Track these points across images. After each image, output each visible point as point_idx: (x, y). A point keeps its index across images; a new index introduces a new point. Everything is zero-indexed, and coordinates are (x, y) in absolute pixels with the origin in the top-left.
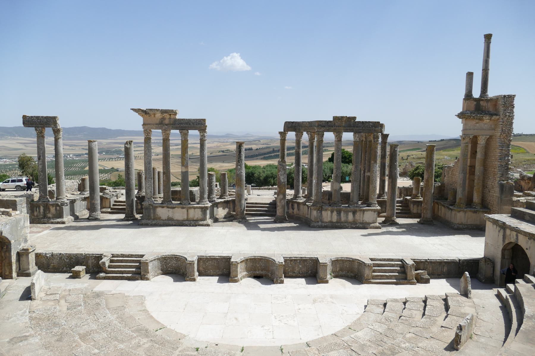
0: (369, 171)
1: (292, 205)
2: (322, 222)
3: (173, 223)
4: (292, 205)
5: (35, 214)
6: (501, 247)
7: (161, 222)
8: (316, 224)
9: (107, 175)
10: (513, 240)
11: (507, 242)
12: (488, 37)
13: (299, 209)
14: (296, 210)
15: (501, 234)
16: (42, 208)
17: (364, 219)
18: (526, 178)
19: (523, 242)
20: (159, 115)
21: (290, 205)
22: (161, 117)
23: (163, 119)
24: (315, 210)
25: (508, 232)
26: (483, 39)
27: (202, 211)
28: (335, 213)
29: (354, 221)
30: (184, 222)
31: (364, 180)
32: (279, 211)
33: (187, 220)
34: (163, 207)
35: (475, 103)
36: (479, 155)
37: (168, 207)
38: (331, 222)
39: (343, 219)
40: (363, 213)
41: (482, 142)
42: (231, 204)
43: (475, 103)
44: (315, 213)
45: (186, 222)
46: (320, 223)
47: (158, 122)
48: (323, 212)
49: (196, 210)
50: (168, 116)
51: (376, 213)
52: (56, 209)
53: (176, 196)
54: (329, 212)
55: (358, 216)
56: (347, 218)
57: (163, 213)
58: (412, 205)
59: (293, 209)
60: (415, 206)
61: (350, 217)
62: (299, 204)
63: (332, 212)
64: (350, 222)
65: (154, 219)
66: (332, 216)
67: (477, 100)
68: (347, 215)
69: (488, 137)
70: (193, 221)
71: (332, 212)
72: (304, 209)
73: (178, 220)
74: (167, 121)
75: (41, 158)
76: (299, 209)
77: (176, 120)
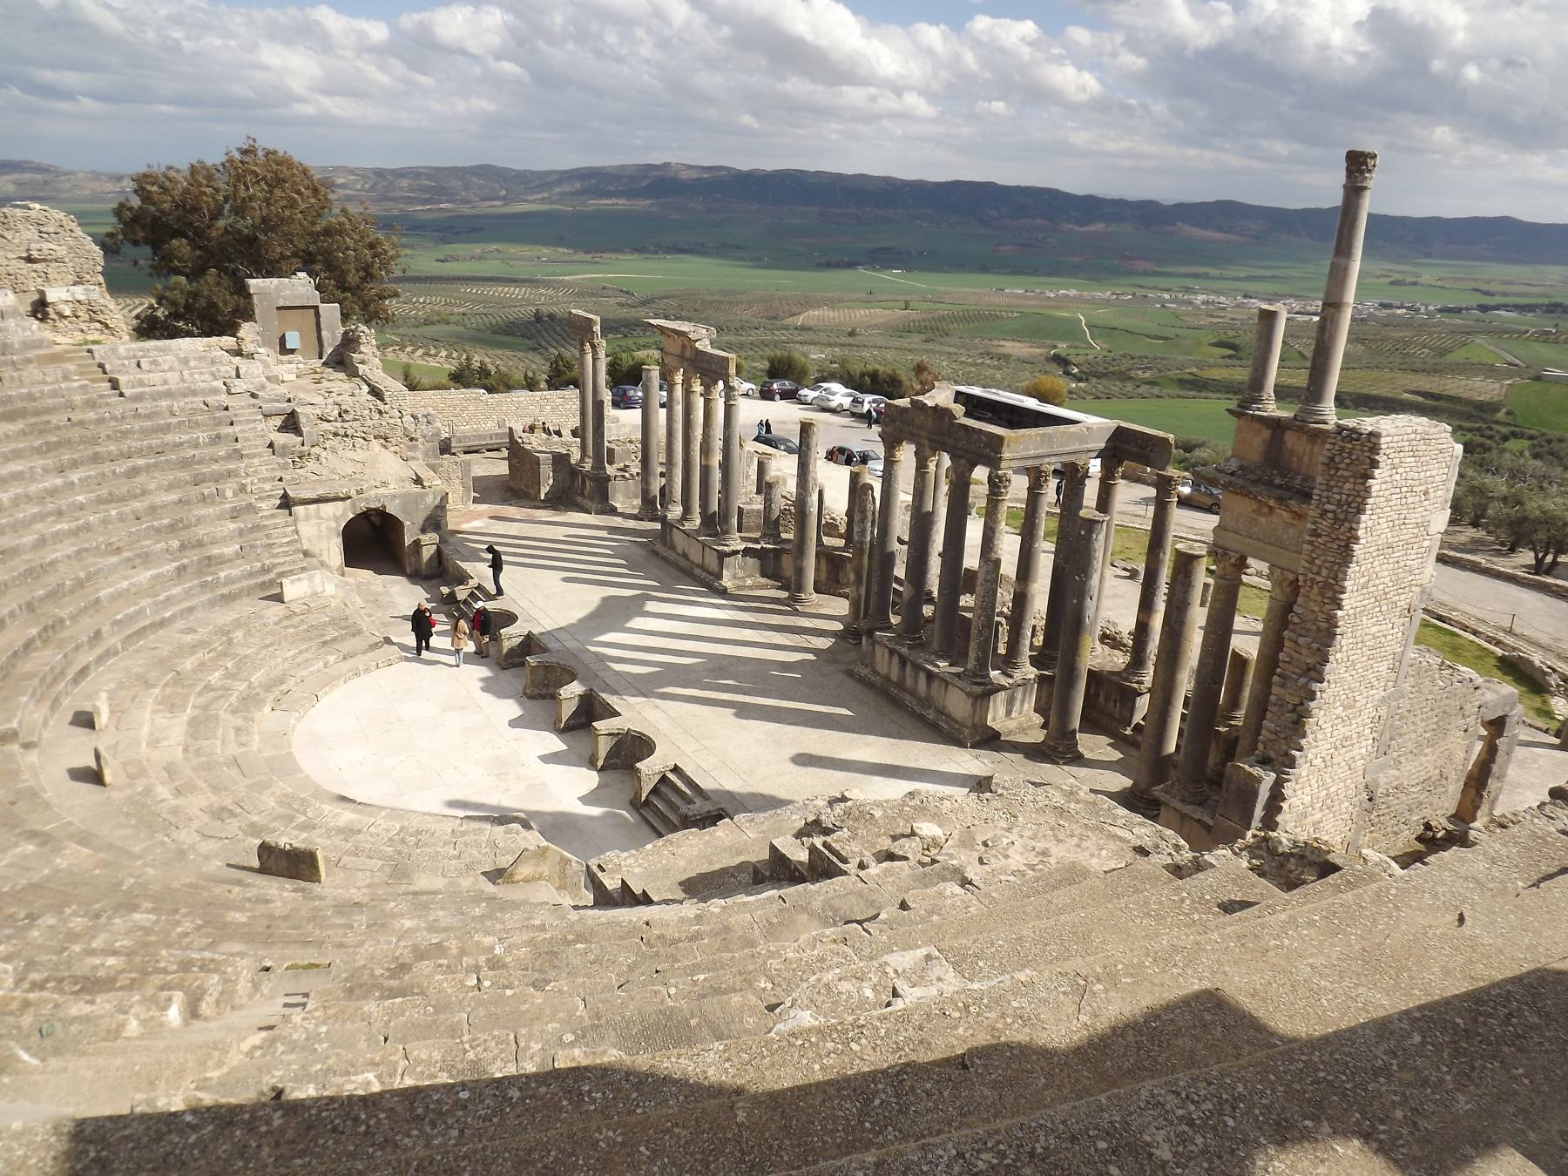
2: (874, 671)
7: (672, 556)
9: (1497, 386)
23: (684, 347)
26: (1341, 177)
28: (896, 660)
35: (1266, 434)
38: (887, 678)
39: (909, 683)
43: (1266, 434)
45: (697, 571)
46: (865, 672)
54: (887, 653)
56: (916, 683)
64: (919, 699)
67: (1276, 425)
71: (892, 652)
74: (688, 353)
77: (699, 353)
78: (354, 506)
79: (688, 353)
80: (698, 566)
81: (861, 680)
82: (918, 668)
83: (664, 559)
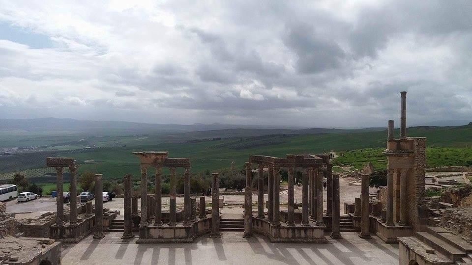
0: (316, 196)
1: (257, 223)
4: (257, 223)
5: (54, 235)
7: (154, 240)
8: (275, 240)
10: (414, 259)
12: (404, 94)
13: (262, 226)
14: (260, 226)
15: (408, 253)
16: (59, 230)
17: (314, 235)
18: (454, 192)
19: (419, 260)
20: (153, 157)
21: (255, 222)
22: (155, 158)
23: (157, 159)
24: (275, 228)
25: (411, 251)
27: (186, 230)
31: (313, 201)
32: (246, 228)
34: (155, 228)
35: (396, 144)
36: (402, 184)
37: (159, 228)
38: (287, 238)
40: (313, 230)
41: (403, 174)
42: (208, 222)
43: (396, 144)
44: (274, 231)
45: (174, 240)
46: (279, 239)
47: (152, 162)
48: (281, 230)
50: (161, 157)
51: (323, 230)
52: (70, 231)
53: (165, 218)
55: (308, 233)
57: (155, 233)
58: (354, 221)
59: (258, 226)
60: (357, 222)
61: (303, 234)
62: (262, 222)
65: (147, 238)
66: (288, 233)
67: (399, 142)
68: (300, 232)
69: (408, 169)
72: (266, 226)
74: (160, 161)
75: (60, 191)
76: (262, 226)
77: (166, 160)
78: (40, 260)
79: (160, 161)
80: (172, 238)
81: (278, 242)
82: (299, 229)
83: (149, 243)
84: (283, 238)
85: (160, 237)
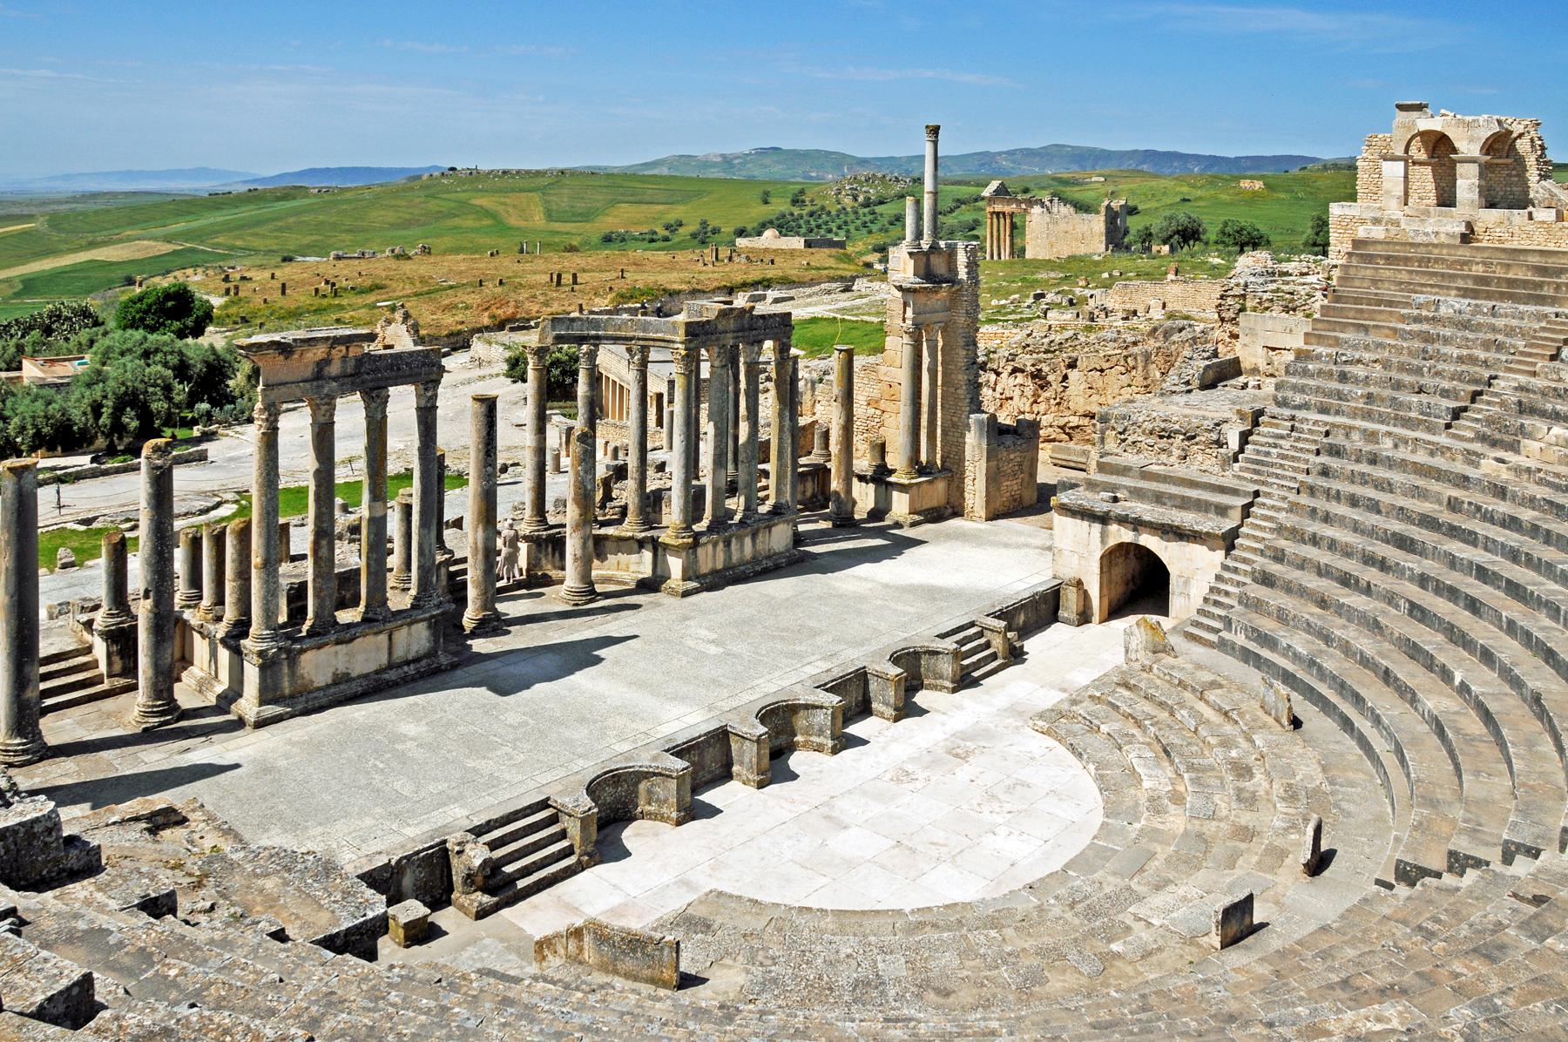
3: (355, 688)
6: (1099, 554)
11: (1112, 542)
19: (1149, 541)
27: (429, 627)
28: (721, 545)
29: (754, 558)
30: (386, 676)
33: (391, 666)
37: (338, 643)
38: (714, 572)
39: (735, 558)
45: (392, 675)
49: (414, 627)
54: (710, 547)
63: (715, 545)
70: (408, 663)
71: (715, 545)
73: (365, 676)
84: (705, 576)
85: (341, 679)
